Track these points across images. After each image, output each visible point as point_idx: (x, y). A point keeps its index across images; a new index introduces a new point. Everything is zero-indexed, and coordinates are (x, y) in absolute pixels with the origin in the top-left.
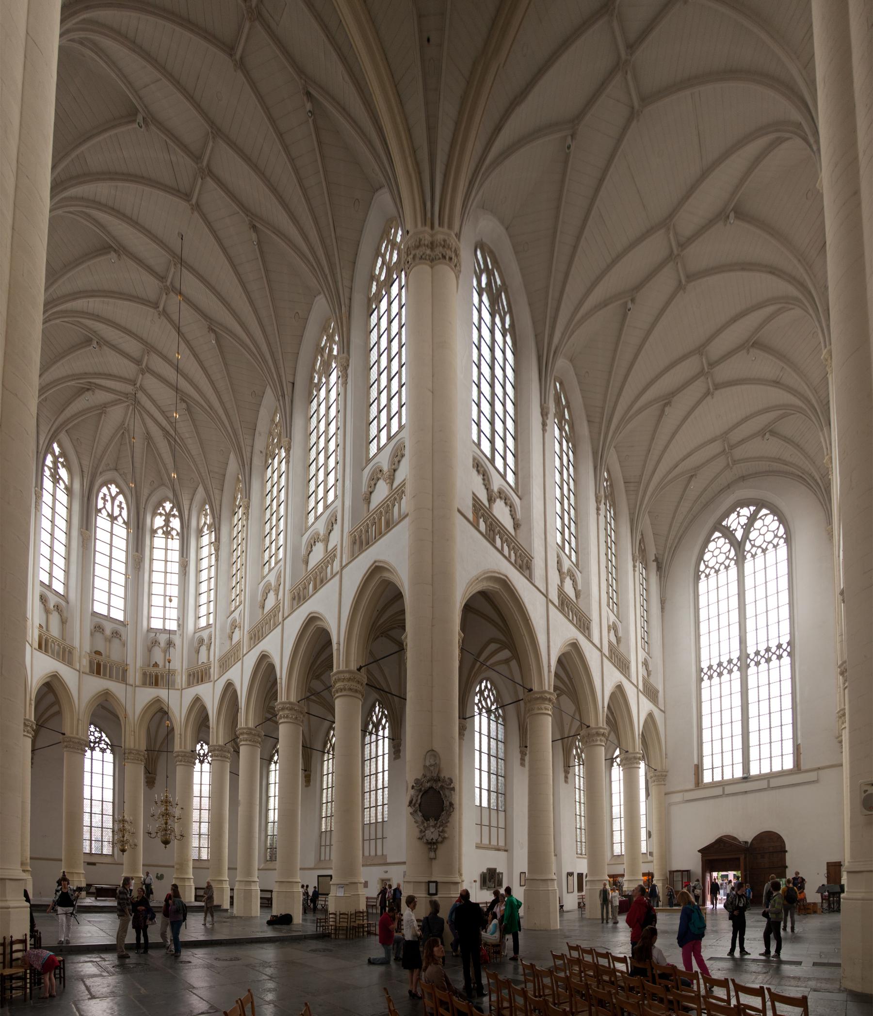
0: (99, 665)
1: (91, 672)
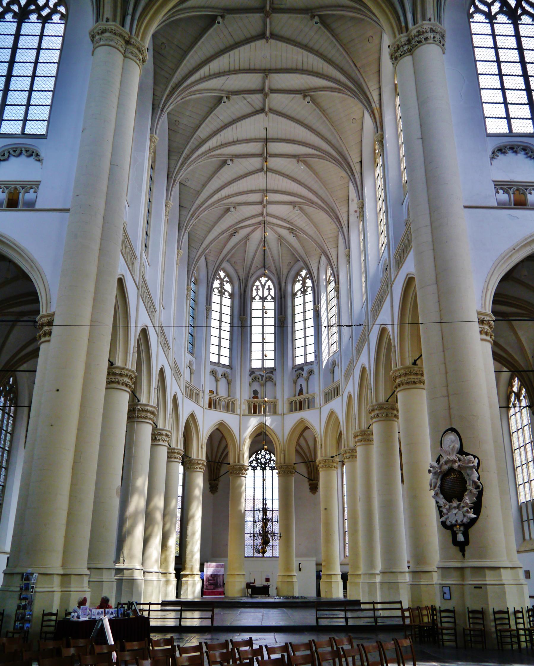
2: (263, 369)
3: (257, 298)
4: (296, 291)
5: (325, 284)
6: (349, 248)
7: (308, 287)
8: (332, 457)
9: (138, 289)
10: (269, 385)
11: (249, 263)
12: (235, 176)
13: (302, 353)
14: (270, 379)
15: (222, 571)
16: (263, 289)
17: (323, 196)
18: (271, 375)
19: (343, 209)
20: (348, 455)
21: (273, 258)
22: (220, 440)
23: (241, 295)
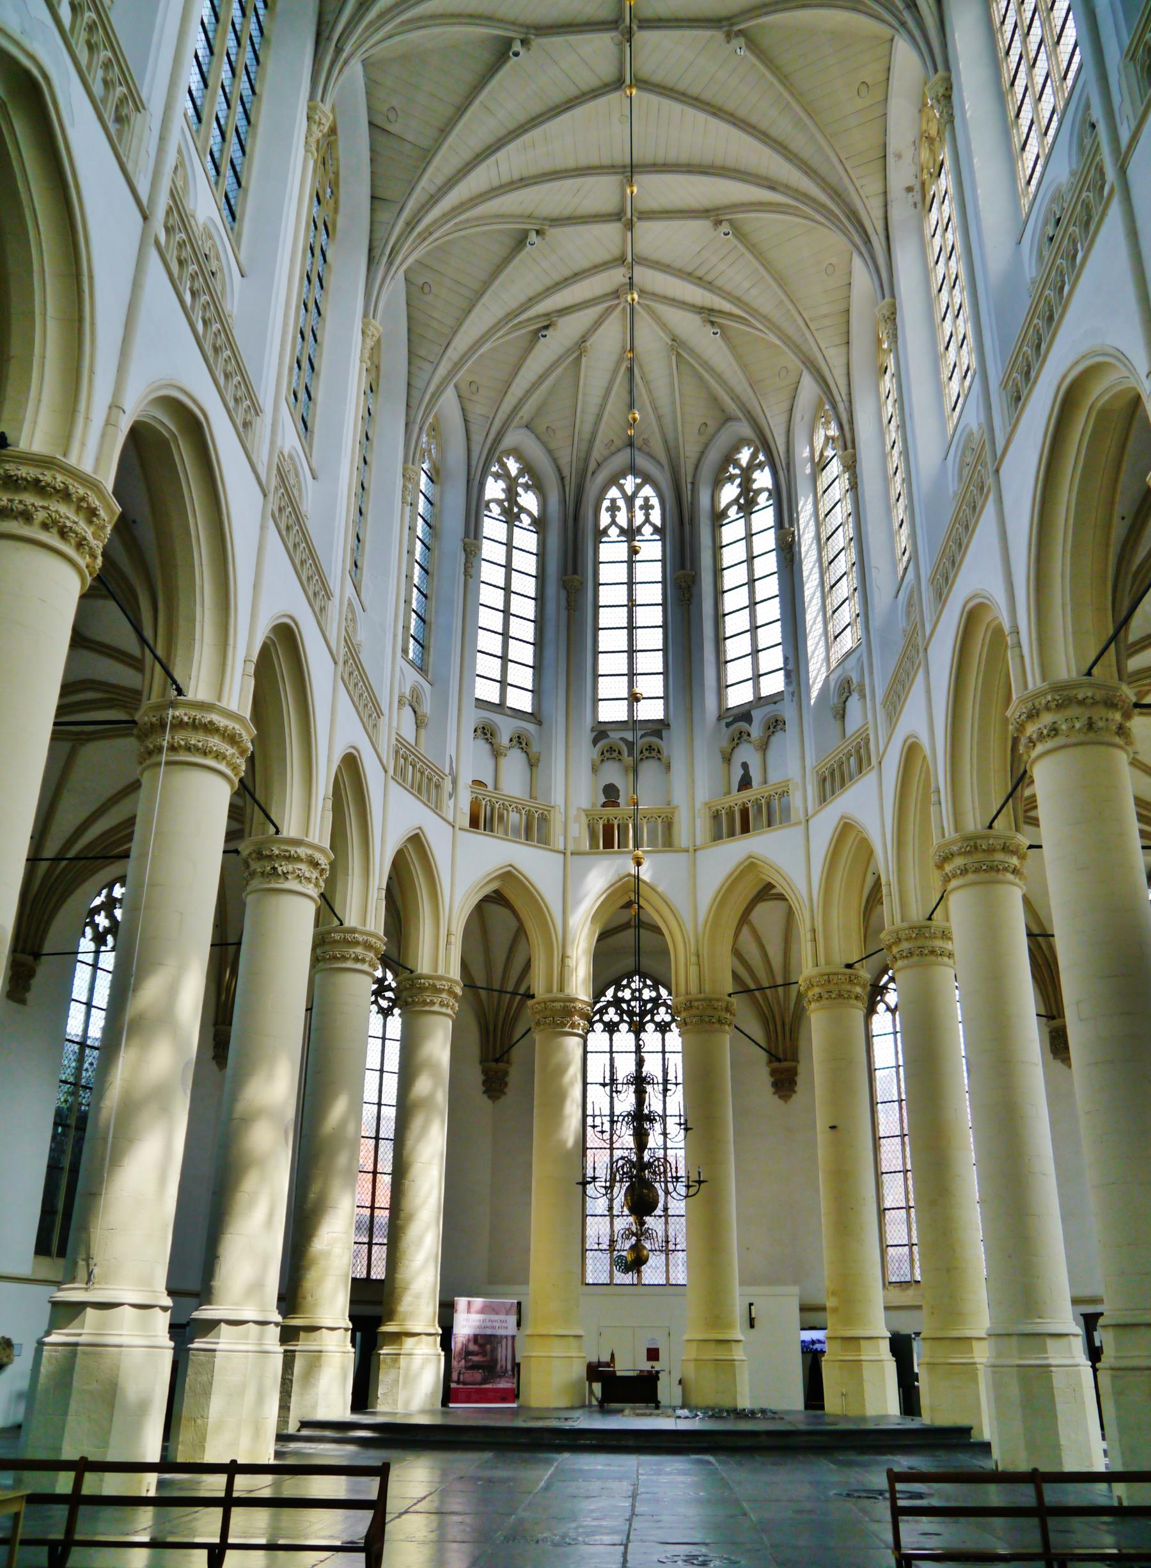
0: (608, 829)
1: (594, 844)
2: (632, 723)
3: (614, 532)
4: (722, 506)
5: (808, 471)
6: (893, 296)
7: (758, 492)
8: (849, 966)
9: (265, 495)
10: (649, 771)
11: (588, 428)
12: (537, 108)
13: (749, 670)
14: (653, 752)
15: (506, 1325)
16: (631, 506)
17: (808, 153)
18: (654, 740)
19: (871, 187)
20: (905, 945)
21: (655, 409)
22: (503, 912)
23: (565, 521)
